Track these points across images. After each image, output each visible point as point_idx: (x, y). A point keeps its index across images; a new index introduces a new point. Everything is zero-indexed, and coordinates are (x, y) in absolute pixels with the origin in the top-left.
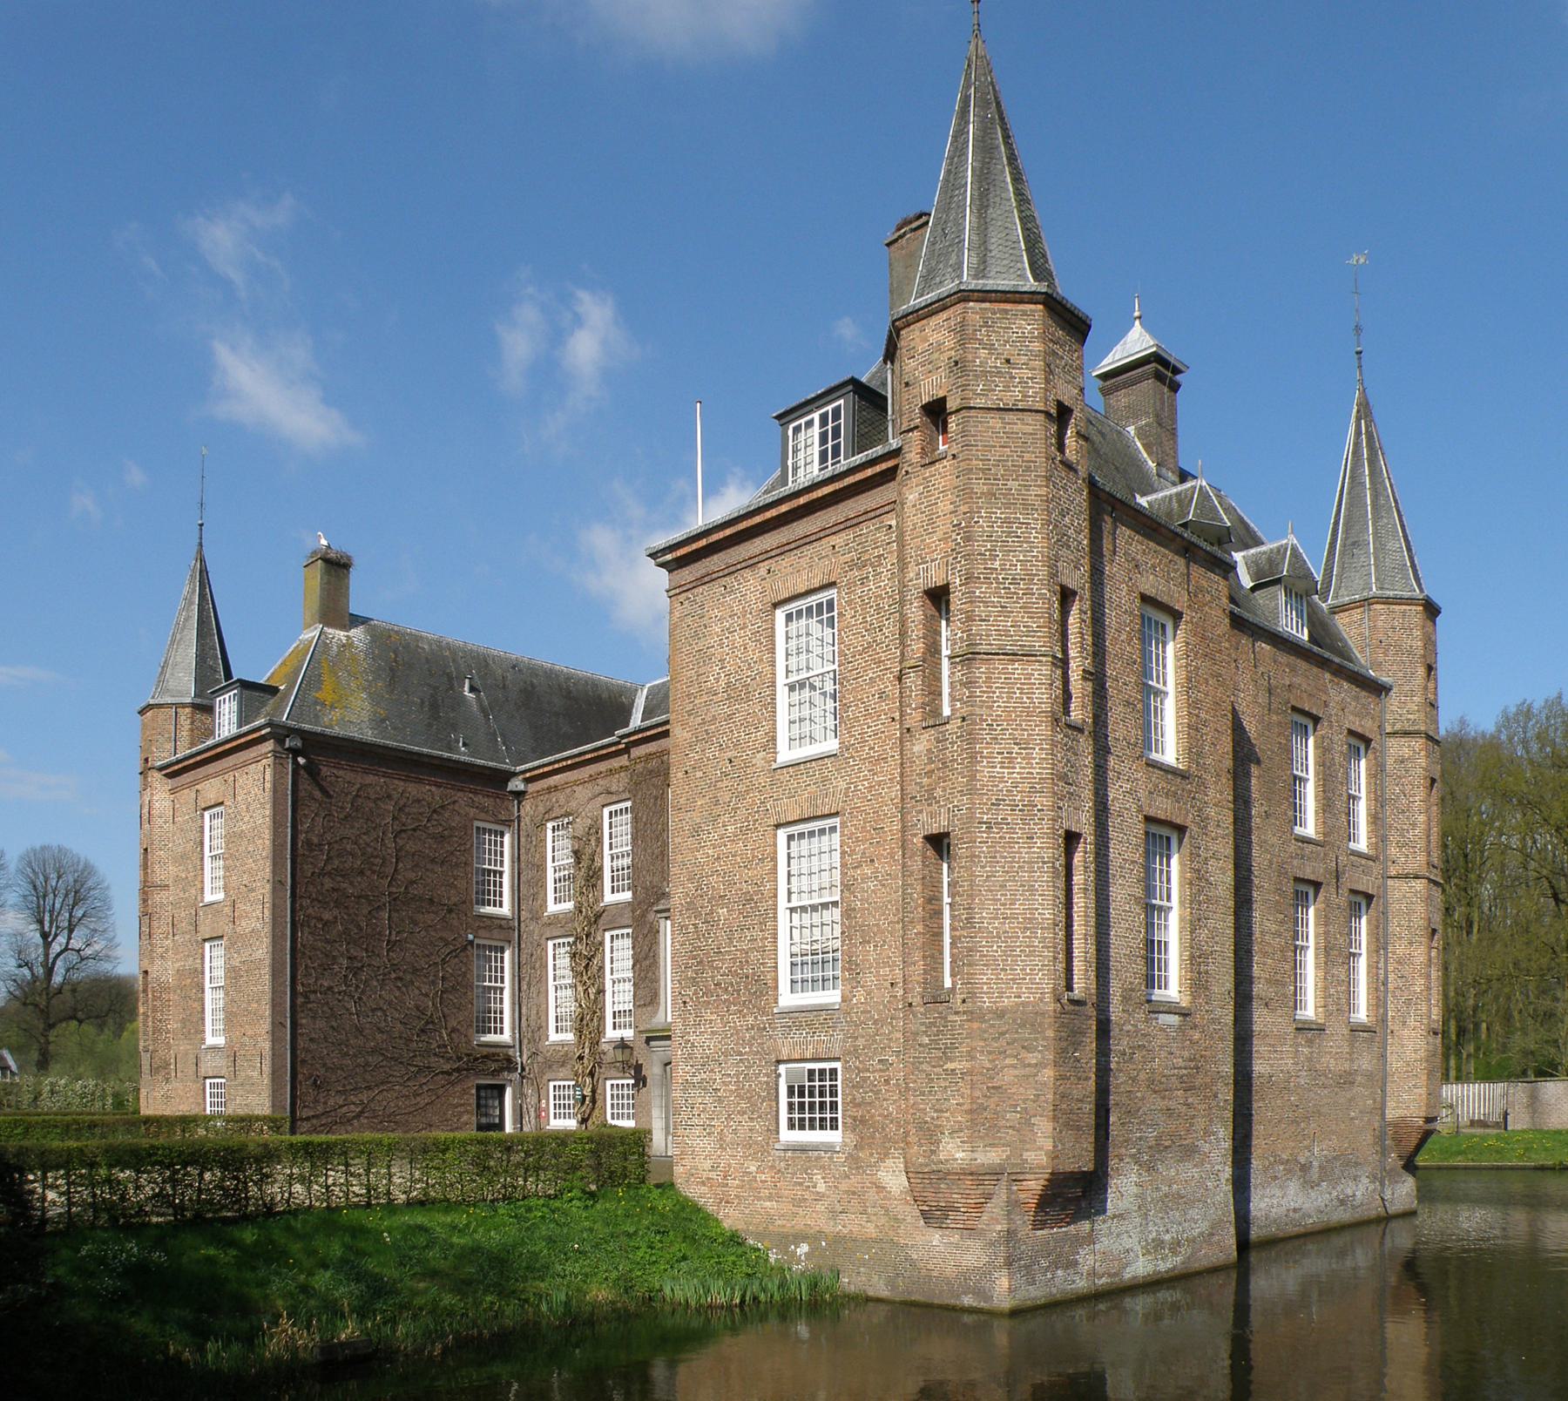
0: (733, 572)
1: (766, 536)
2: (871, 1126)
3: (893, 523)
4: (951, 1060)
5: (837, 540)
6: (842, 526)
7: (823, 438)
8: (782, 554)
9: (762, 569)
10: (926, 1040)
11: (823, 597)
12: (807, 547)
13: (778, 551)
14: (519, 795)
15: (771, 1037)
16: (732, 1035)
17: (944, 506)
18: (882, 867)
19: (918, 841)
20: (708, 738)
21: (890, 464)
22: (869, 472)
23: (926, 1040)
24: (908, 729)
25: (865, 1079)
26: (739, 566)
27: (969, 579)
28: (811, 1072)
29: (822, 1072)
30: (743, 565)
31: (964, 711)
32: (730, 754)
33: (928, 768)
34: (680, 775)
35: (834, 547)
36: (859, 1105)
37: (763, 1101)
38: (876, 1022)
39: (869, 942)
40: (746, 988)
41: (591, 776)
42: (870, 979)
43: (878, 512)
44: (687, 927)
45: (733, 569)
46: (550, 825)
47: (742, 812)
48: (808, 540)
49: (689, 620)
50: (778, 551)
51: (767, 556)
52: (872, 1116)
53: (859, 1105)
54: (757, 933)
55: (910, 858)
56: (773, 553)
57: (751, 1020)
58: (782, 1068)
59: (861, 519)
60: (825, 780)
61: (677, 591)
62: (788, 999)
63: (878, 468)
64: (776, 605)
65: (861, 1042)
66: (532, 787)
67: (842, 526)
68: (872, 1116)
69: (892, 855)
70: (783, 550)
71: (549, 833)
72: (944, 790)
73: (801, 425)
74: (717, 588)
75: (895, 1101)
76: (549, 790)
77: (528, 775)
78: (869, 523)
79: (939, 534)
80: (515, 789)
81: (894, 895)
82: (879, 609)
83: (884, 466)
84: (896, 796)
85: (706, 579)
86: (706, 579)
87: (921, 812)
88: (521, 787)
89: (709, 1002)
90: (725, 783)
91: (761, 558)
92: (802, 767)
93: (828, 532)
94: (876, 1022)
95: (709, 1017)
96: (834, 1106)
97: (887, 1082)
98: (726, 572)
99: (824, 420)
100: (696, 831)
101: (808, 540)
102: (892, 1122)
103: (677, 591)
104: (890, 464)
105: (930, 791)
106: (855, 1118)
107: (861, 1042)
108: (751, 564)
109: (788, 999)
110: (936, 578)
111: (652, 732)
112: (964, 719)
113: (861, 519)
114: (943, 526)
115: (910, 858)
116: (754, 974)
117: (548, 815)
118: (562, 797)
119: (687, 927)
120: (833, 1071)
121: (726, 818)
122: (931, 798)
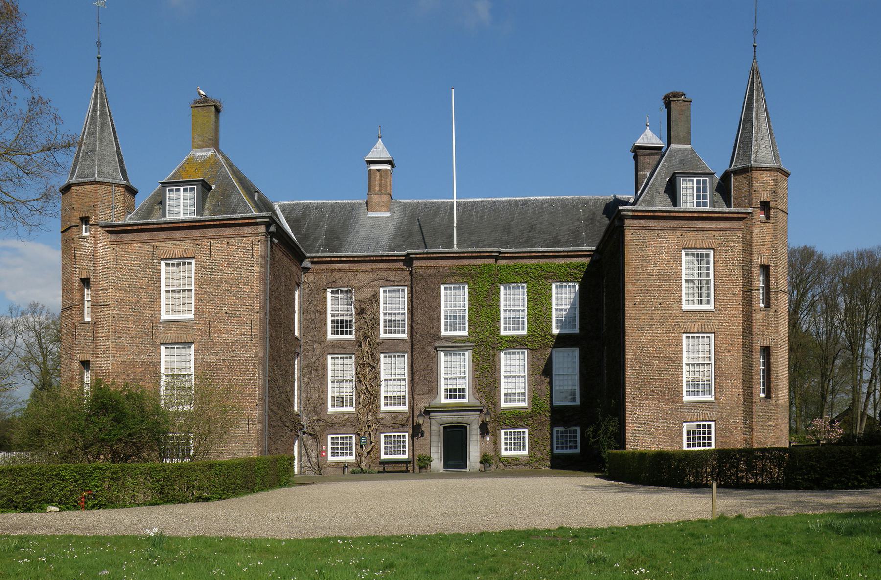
0: (663, 230)
1: (681, 221)
2: (729, 444)
3: (741, 235)
4: (770, 421)
5: (717, 234)
6: (718, 229)
7: (698, 190)
8: (689, 230)
9: (679, 233)
10: (761, 414)
11: (705, 252)
12: (701, 232)
13: (688, 229)
14: (307, 269)
15: (681, 412)
16: (660, 411)
17: (769, 238)
18: (734, 354)
19: (758, 348)
20: (647, 292)
21: (745, 216)
22: (736, 215)
23: (761, 414)
24: (755, 310)
25: (726, 428)
26: (666, 229)
27: (776, 266)
28: (699, 426)
29: (704, 425)
30: (669, 229)
31: (776, 308)
32: (660, 301)
33: (762, 324)
34: (631, 304)
35: (714, 236)
36: (724, 437)
37: (678, 437)
38: (731, 408)
39: (728, 379)
40: (668, 393)
41: (372, 269)
42: (728, 393)
43: (735, 230)
44: (635, 367)
45: (663, 229)
46: (329, 290)
47: (666, 325)
48: (702, 229)
49: (637, 242)
50: (688, 229)
51: (681, 229)
52: (730, 441)
53: (724, 437)
54: (674, 372)
55: (755, 353)
56: (685, 229)
57: (671, 405)
58: (684, 424)
59: (727, 230)
60: (708, 319)
61: (631, 228)
62: (686, 398)
63: (739, 215)
64: (684, 249)
65: (724, 415)
66: (314, 267)
67: (718, 229)
68: (730, 441)
69: (738, 350)
70: (690, 229)
71: (329, 295)
72: (768, 332)
73: (687, 180)
74: (654, 234)
75: (739, 435)
76: (333, 271)
77: (315, 259)
78: (730, 232)
79: (766, 247)
80: (306, 266)
81: (739, 364)
82: (733, 264)
83: (742, 215)
84: (740, 330)
85: (648, 228)
86: (648, 228)
87: (759, 338)
88: (309, 265)
89: (648, 398)
90: (657, 312)
91: (679, 229)
92: (697, 312)
93: (712, 229)
94: (731, 408)
95: (647, 404)
96: (710, 438)
97: (736, 429)
98: (659, 228)
99: (698, 182)
100: (641, 329)
101: (702, 229)
102: (738, 443)
103: (631, 228)
104: (745, 216)
105: (763, 332)
106: (722, 442)
107: (724, 415)
108: (673, 230)
109: (686, 398)
110: (765, 261)
111: (435, 255)
112: (775, 311)
113: (727, 230)
114: (768, 245)
115: (755, 353)
116: (673, 388)
117: (332, 284)
118: (344, 277)
119: (635, 367)
120: (710, 426)
121: (658, 326)
122: (763, 335)
